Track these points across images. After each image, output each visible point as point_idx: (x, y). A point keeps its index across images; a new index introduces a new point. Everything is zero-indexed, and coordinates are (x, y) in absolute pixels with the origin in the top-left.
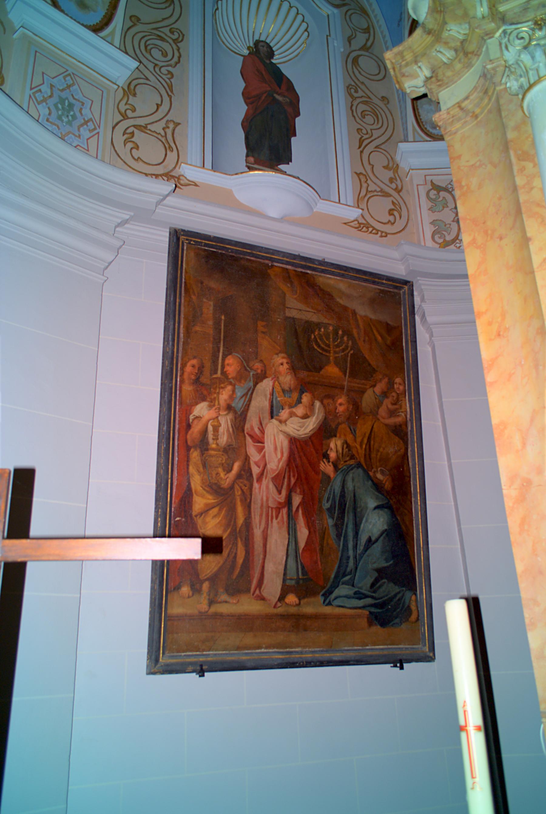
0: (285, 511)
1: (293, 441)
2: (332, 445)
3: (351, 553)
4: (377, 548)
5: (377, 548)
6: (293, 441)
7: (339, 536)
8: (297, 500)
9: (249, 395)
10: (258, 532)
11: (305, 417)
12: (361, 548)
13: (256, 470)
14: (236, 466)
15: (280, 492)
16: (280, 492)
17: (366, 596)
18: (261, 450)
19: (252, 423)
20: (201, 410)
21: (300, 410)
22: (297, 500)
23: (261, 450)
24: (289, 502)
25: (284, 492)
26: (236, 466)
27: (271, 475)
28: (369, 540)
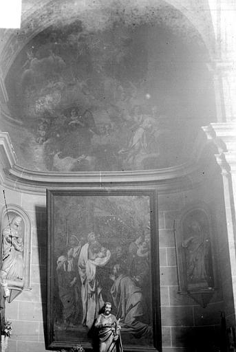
0: (95, 295)
1: (98, 268)
2: (115, 268)
3: (123, 310)
4: (134, 310)
5: (134, 310)
6: (98, 268)
7: (118, 303)
8: (99, 290)
9: (79, 252)
10: (84, 302)
11: (103, 257)
12: (128, 308)
13: (82, 280)
14: (75, 279)
15: (92, 288)
16: (92, 288)
17: (129, 327)
18: (84, 272)
19: (80, 262)
20: (61, 259)
21: (101, 254)
22: (99, 290)
23: (84, 272)
24: (96, 292)
25: (94, 287)
26: (75, 279)
27: (89, 281)
28: (132, 305)
